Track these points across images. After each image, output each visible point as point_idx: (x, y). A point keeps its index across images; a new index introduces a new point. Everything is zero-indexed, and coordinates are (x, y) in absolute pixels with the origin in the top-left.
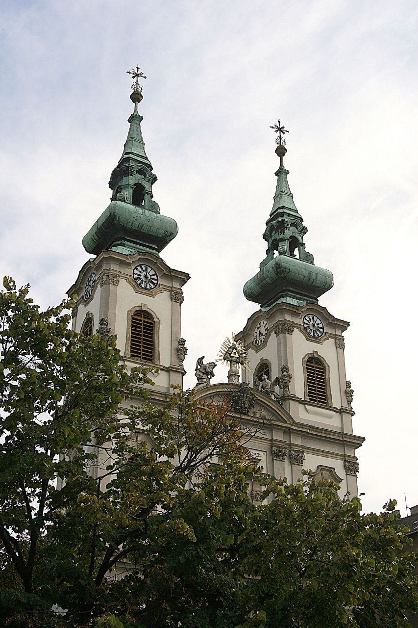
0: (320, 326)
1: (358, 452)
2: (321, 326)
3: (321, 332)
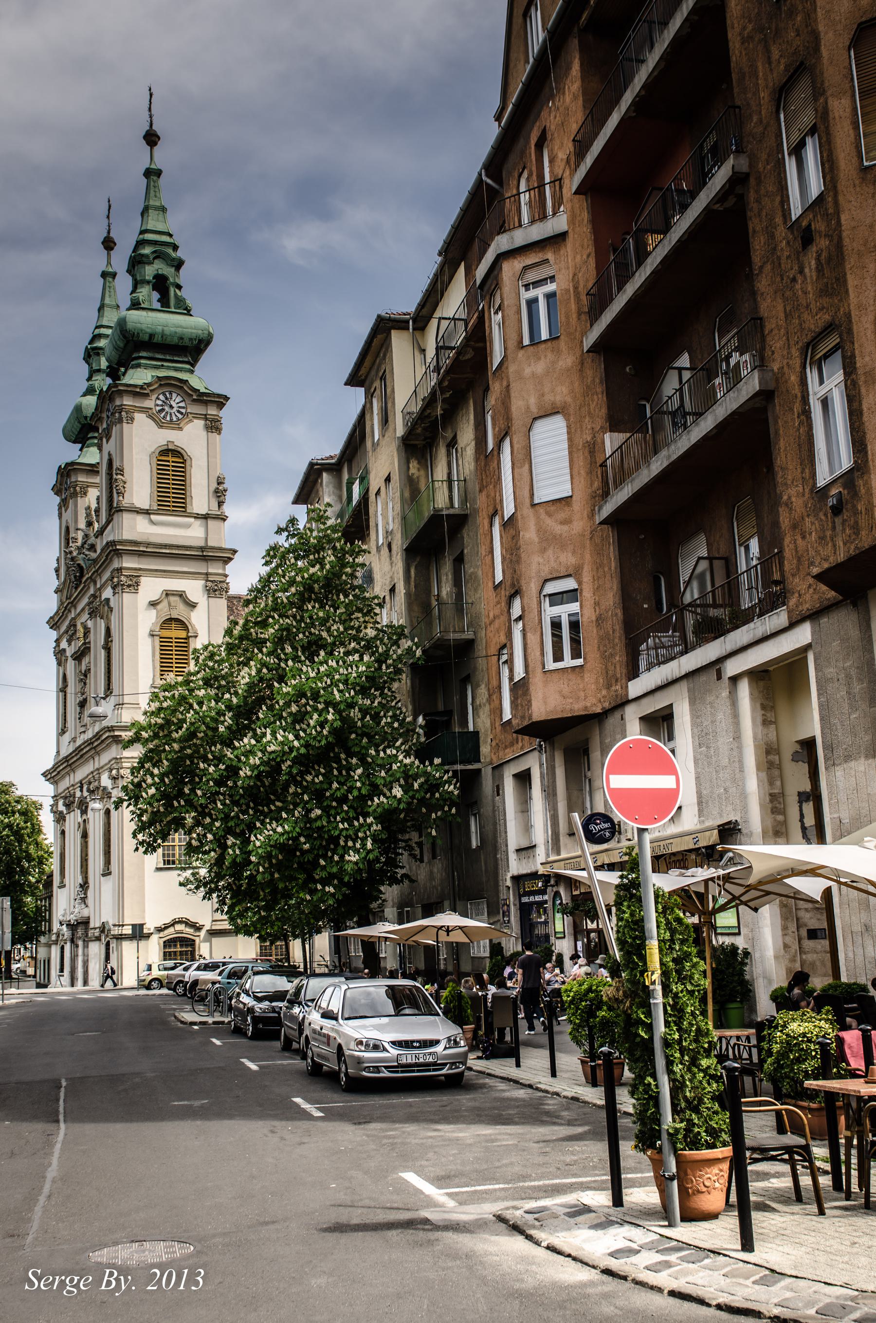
0: (181, 405)
1: (230, 568)
2: (182, 404)
3: (182, 413)
